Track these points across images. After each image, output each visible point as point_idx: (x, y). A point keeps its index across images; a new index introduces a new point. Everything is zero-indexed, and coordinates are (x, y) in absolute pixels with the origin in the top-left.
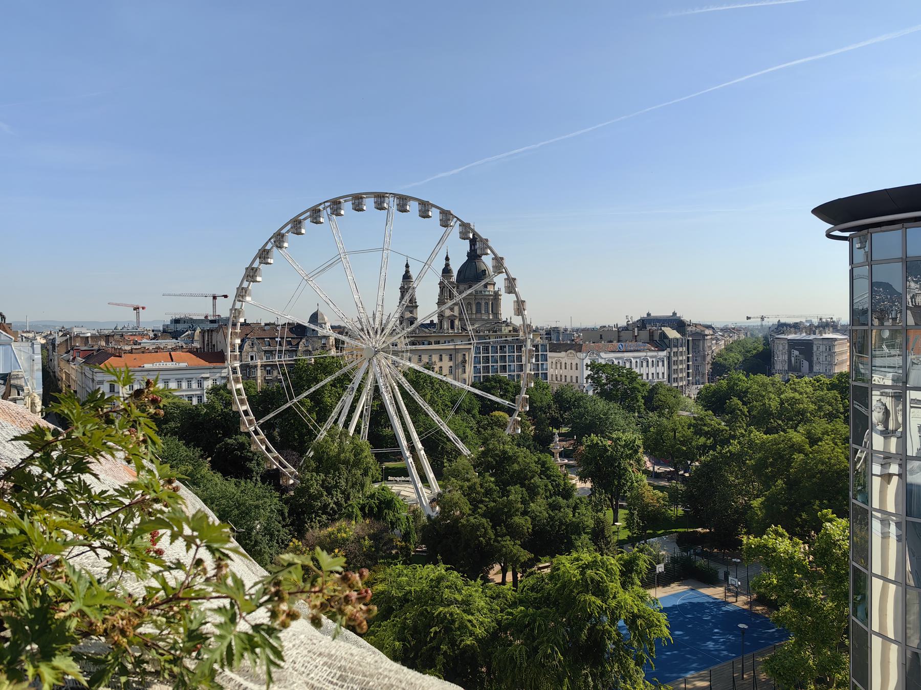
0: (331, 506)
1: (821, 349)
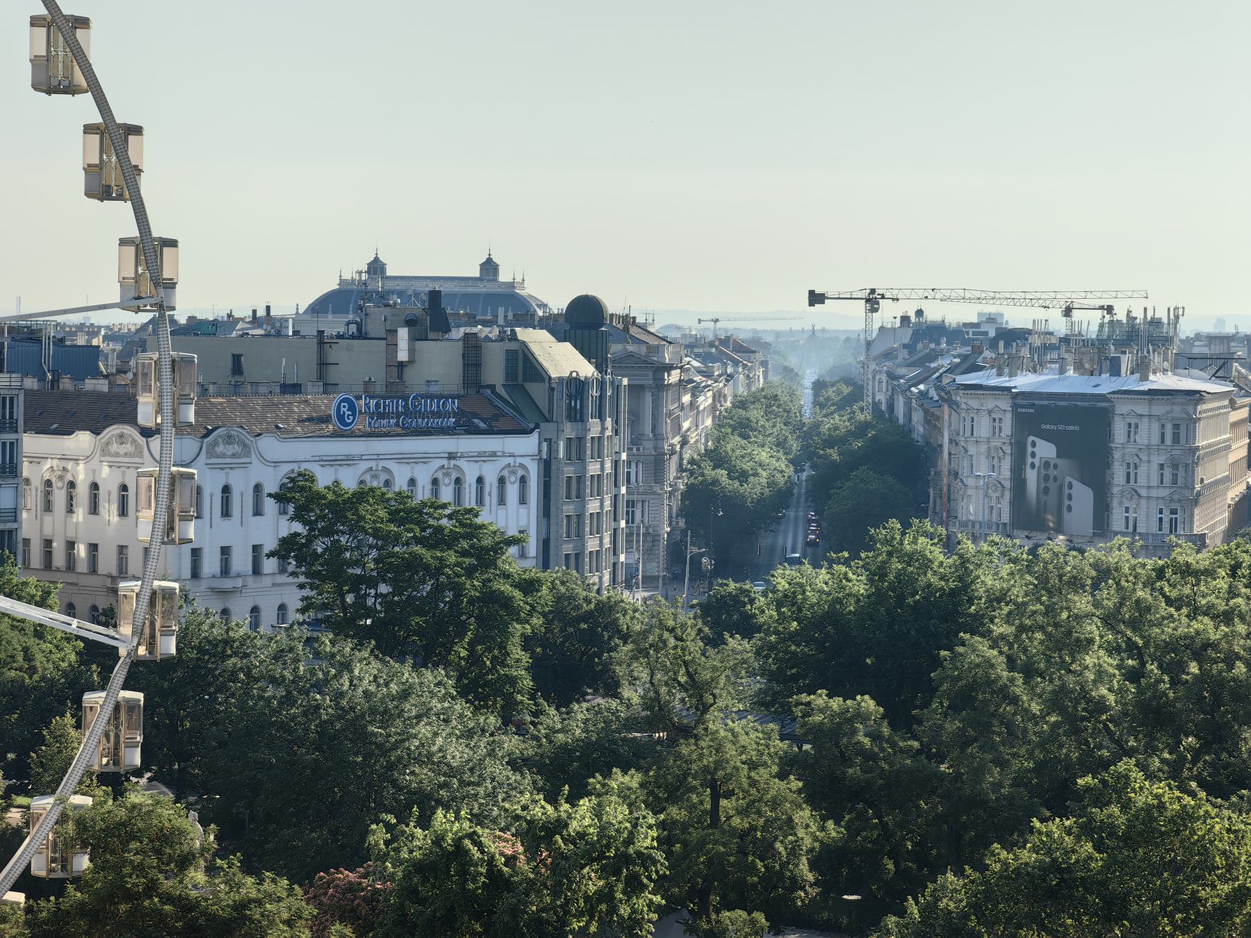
1: (1142, 438)
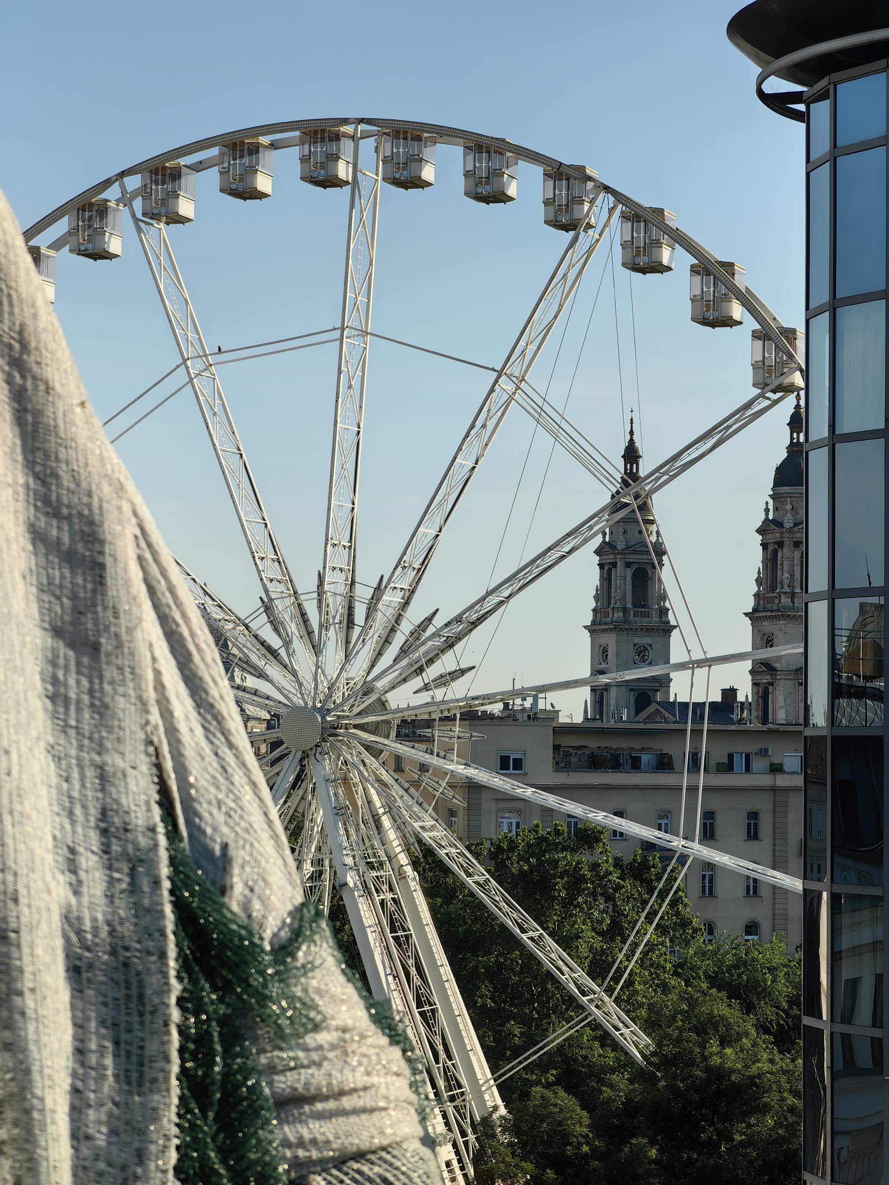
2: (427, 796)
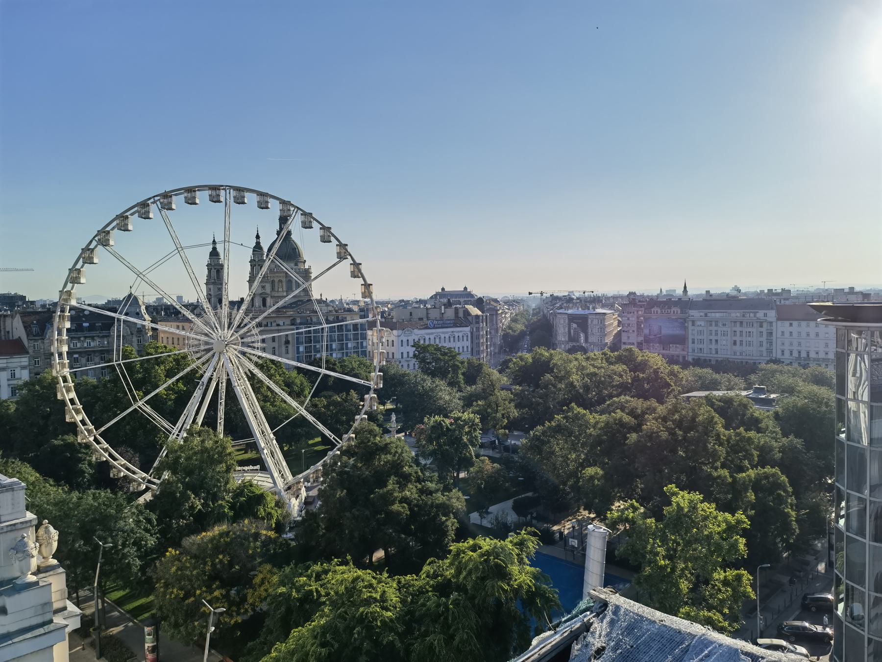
0: (199, 507)
1: (594, 323)
2: (251, 360)
